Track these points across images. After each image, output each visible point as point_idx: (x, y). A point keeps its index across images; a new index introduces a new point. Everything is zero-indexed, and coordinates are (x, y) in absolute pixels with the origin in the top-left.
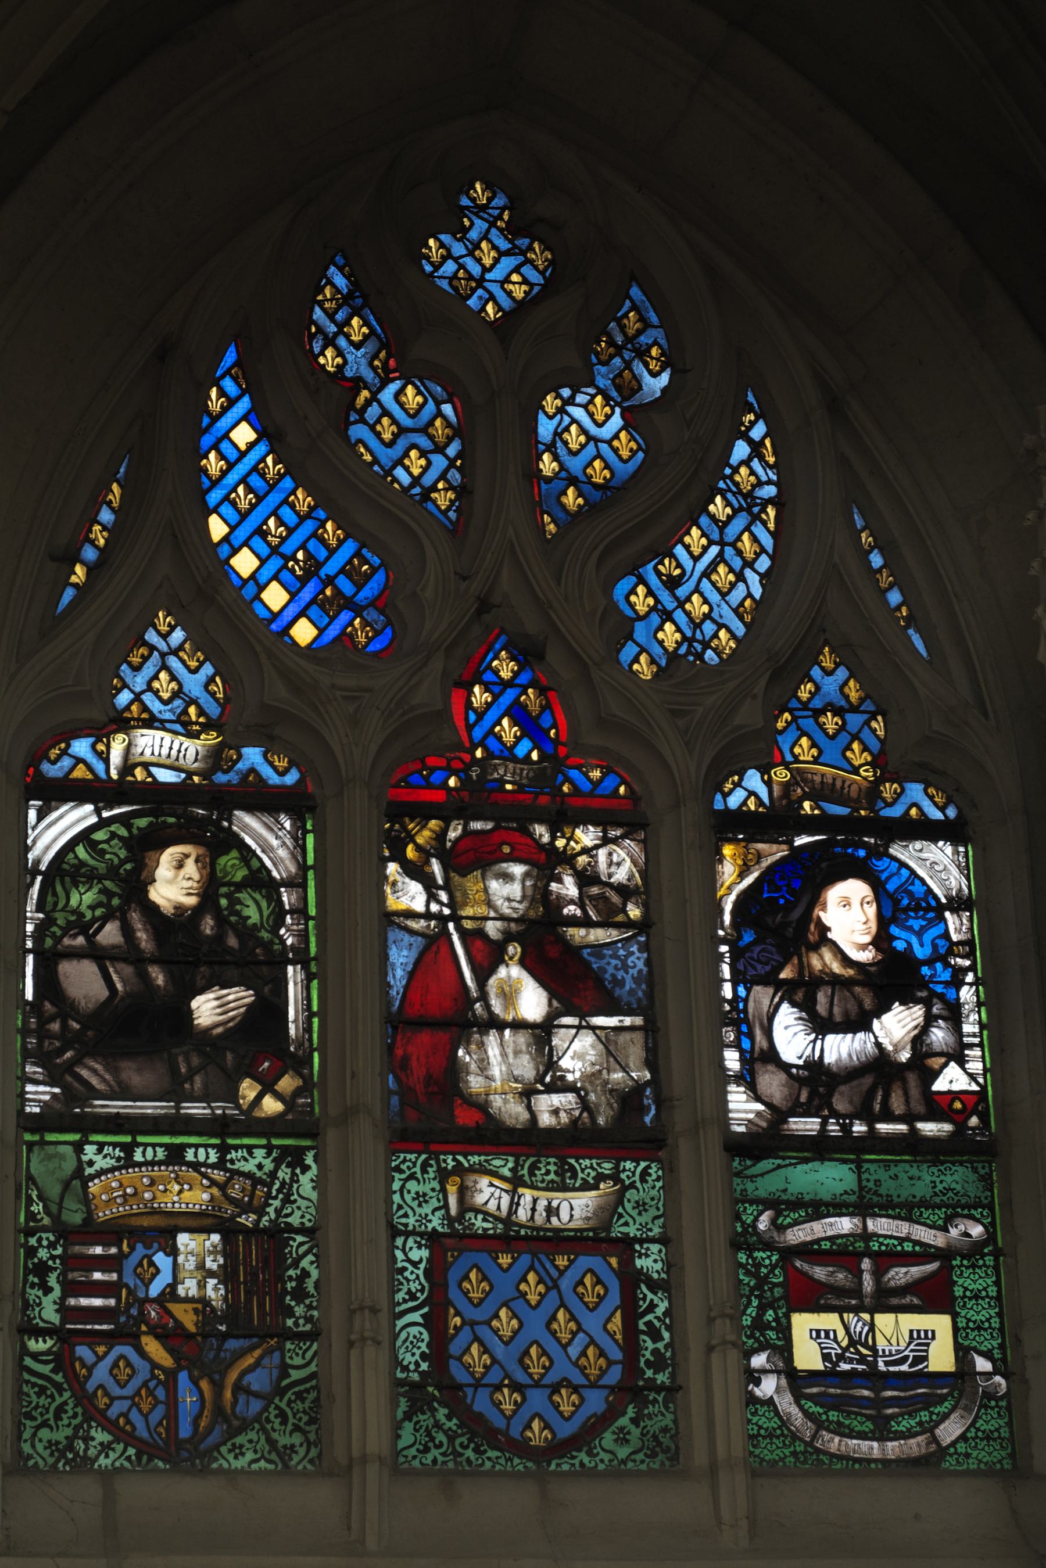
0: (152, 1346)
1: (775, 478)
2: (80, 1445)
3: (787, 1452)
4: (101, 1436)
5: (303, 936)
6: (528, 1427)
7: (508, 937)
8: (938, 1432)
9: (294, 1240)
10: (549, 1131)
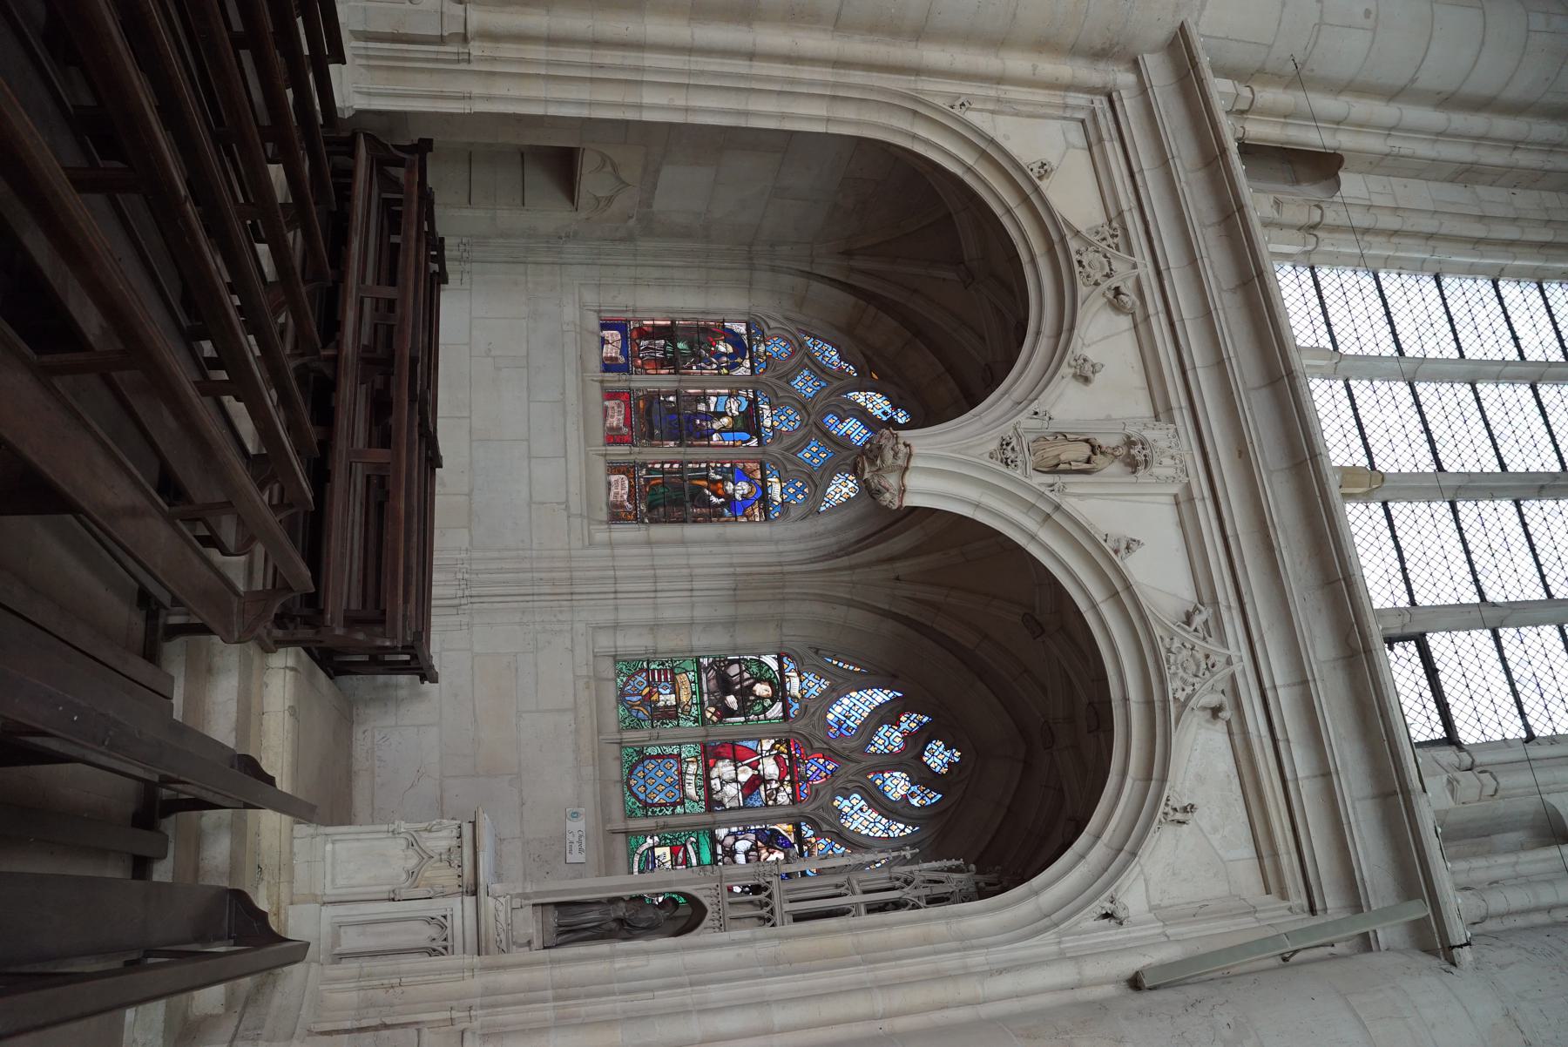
0: (647, 690)
4: (625, 679)
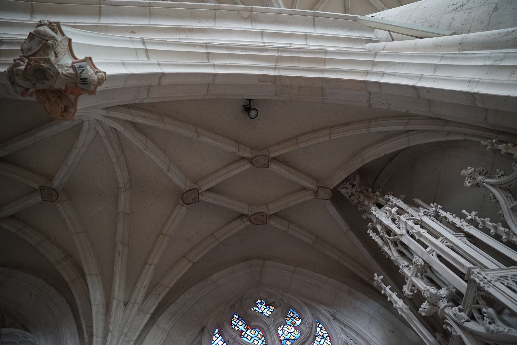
1: (326, 332)
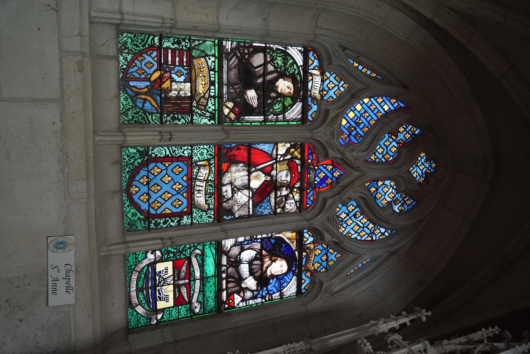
0: (157, 74)
1: (377, 239)
2: (126, 51)
3: (131, 263)
4: (129, 58)
5: (271, 121)
6: (136, 187)
7: (272, 177)
8: (139, 306)
9: (189, 117)
10: (221, 190)
